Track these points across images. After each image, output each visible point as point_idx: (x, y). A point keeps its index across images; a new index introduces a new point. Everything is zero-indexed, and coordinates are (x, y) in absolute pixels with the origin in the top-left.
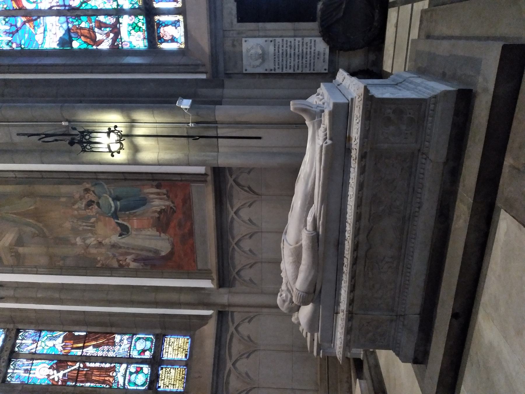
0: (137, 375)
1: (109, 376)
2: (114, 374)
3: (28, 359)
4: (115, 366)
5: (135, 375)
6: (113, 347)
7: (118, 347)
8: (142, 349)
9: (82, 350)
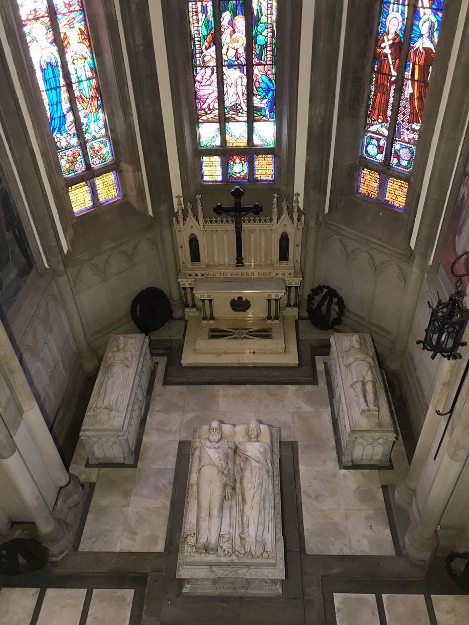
2: (380, 121)
5: (377, 144)
9: (410, 78)
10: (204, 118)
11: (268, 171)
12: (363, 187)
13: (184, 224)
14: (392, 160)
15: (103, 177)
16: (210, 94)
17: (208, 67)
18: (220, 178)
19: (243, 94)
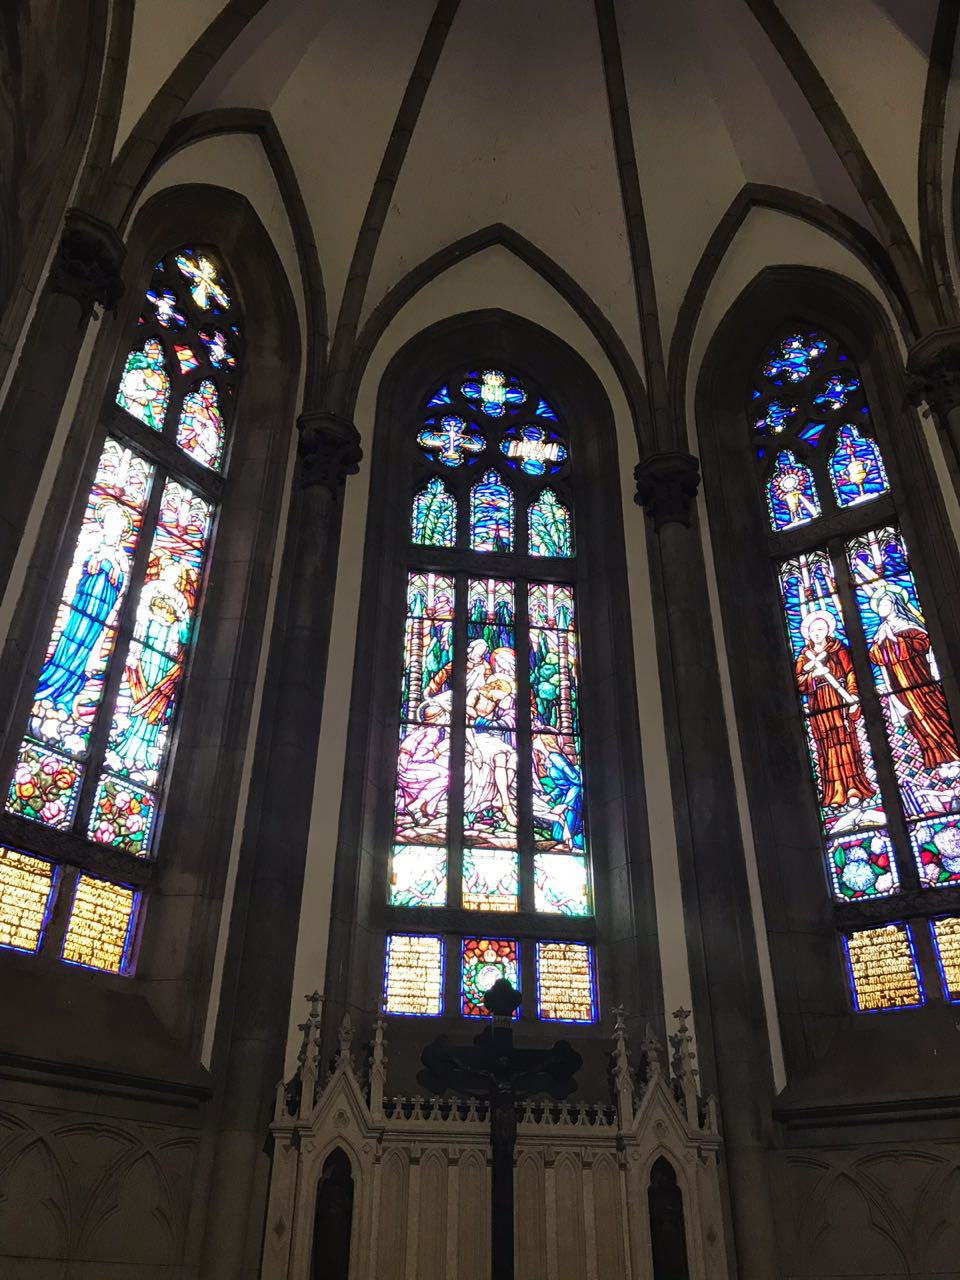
0: (867, 862)
1: (845, 792)
2: (854, 801)
3: (836, 579)
4: (874, 793)
5: (865, 856)
6: (923, 768)
7: (927, 783)
8: (939, 853)
9: (891, 690)
10: (408, 833)
11: (576, 992)
12: (867, 988)
13: (315, 1103)
14: (922, 875)
15: (103, 888)
16: (430, 780)
17: (433, 725)
18: (434, 1008)
19: (509, 787)
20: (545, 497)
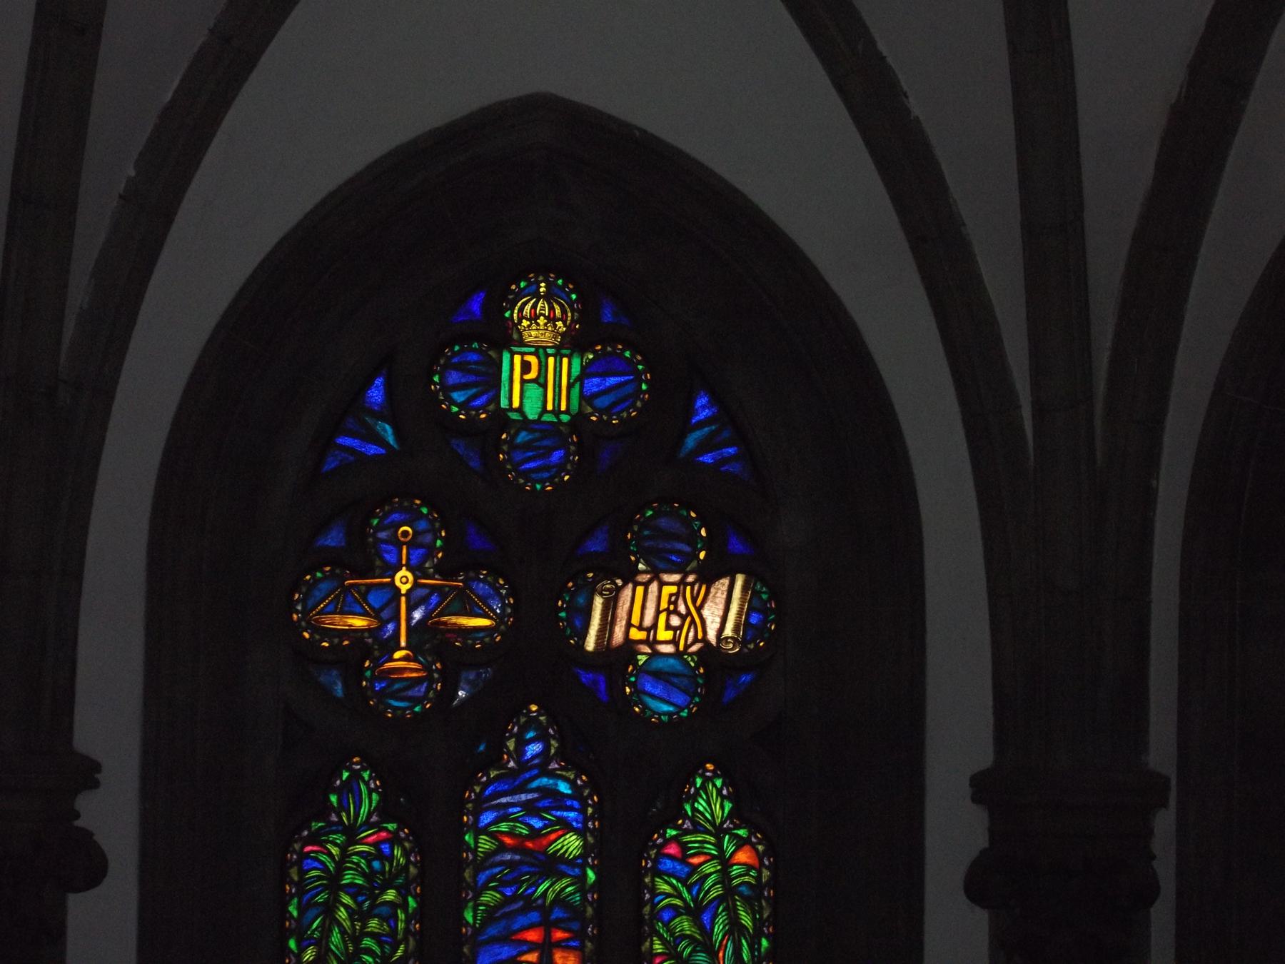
20: (701, 805)
